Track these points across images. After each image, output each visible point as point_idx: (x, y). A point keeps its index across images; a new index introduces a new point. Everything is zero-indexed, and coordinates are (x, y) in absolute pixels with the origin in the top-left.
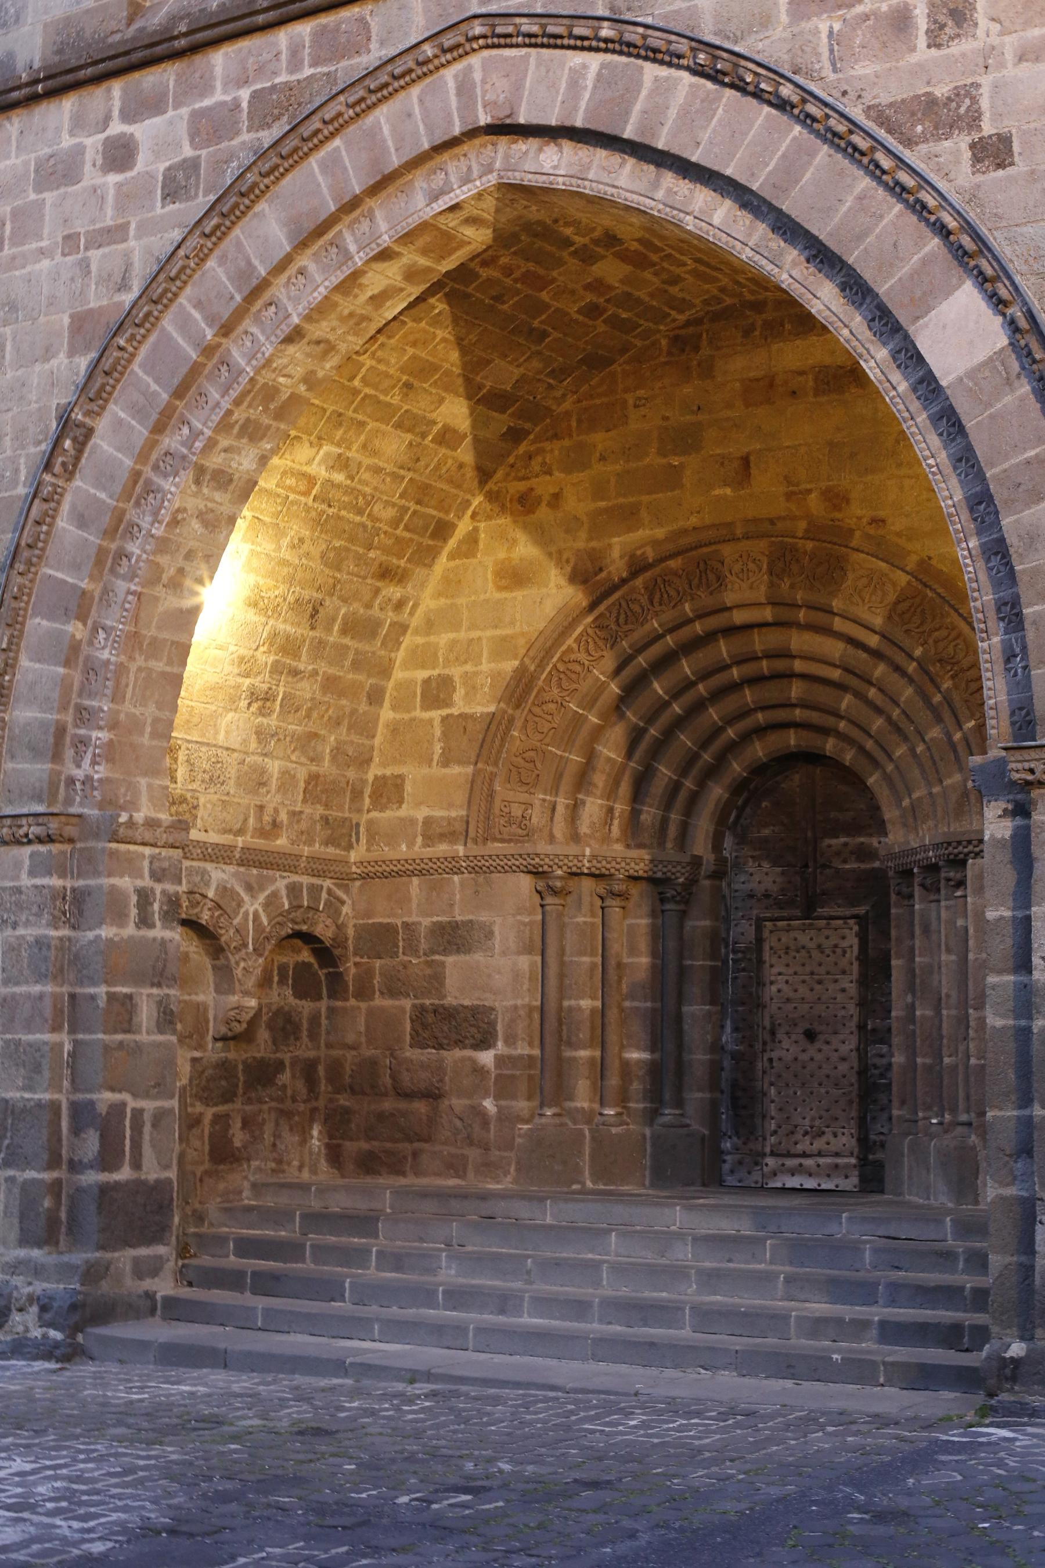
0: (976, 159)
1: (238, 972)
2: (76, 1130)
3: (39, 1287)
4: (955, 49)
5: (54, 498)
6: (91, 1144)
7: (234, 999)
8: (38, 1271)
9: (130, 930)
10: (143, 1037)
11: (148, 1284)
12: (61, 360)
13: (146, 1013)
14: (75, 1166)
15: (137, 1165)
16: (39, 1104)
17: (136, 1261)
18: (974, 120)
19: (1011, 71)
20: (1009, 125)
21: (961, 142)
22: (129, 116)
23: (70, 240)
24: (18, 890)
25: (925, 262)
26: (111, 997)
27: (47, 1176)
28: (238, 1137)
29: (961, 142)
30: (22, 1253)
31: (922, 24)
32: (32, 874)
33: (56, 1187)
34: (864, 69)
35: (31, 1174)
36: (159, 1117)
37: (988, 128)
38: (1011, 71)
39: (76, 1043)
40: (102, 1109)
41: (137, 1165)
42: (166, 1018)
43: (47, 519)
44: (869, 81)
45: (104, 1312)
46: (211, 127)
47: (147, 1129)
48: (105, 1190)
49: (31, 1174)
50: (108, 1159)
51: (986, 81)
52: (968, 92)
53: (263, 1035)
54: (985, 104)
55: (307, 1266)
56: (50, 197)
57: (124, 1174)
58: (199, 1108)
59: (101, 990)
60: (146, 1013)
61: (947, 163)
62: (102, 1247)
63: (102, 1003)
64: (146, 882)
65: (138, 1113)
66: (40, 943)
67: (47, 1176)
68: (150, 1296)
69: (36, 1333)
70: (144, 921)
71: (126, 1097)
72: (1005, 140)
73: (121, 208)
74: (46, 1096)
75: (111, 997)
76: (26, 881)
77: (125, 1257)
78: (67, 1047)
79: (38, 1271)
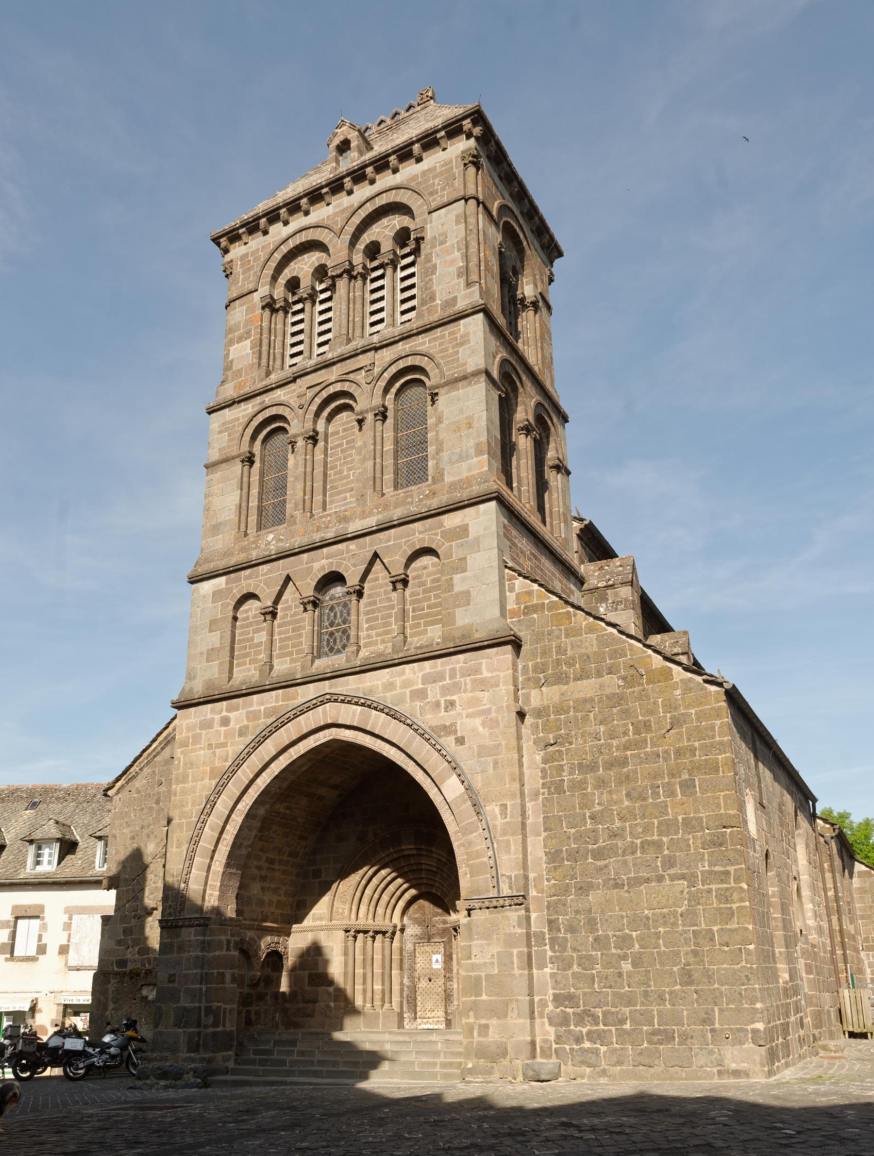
0: (456, 743)
1: (255, 964)
2: (206, 1015)
3: (193, 1066)
4: (451, 713)
5: (204, 822)
6: (211, 1019)
7: (251, 973)
8: (193, 1060)
9: (224, 952)
10: (227, 985)
11: (226, 1064)
12: (206, 781)
13: (228, 978)
14: (205, 1027)
15: (224, 1026)
16: (195, 1007)
17: (223, 1056)
18: (456, 732)
19: (465, 720)
20: (464, 734)
21: (451, 739)
22: (228, 710)
23: (210, 745)
24: (190, 941)
25: (444, 769)
26: (218, 973)
27: (196, 1030)
28: (253, 1017)
29: (451, 739)
30: (188, 1055)
31: (443, 705)
32: (195, 936)
33: (199, 1033)
34: (429, 716)
35: (191, 1030)
36: (231, 1010)
37: (459, 734)
38: (465, 720)
39: (207, 988)
40: (214, 1008)
41: (224, 1026)
42: (234, 980)
43: (202, 829)
44: (428, 720)
45: (215, 1072)
46: (253, 716)
47: (227, 1014)
48: (214, 1033)
49: (191, 1030)
50: (216, 1024)
51: (459, 722)
52: (454, 724)
53: (262, 984)
54: (458, 728)
55: (276, 1056)
56: (204, 732)
57: (220, 1029)
58: (242, 1008)
59: (215, 971)
60: (228, 978)
61: (448, 742)
62: (213, 1052)
63: (215, 975)
64: (229, 937)
65: (225, 1009)
66: (197, 957)
67: (196, 1030)
68: (227, 1068)
69: (193, 1080)
70: (228, 949)
71: (221, 1004)
72: (463, 738)
73: (225, 737)
74: (197, 1005)
75: (218, 973)
76: (193, 938)
77: (220, 1055)
78: (204, 989)
79: (193, 1060)
